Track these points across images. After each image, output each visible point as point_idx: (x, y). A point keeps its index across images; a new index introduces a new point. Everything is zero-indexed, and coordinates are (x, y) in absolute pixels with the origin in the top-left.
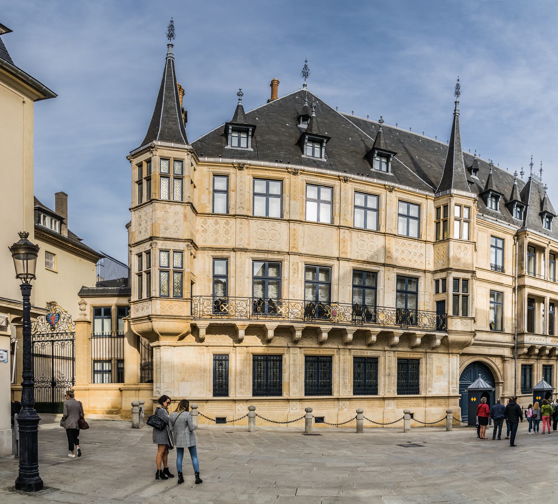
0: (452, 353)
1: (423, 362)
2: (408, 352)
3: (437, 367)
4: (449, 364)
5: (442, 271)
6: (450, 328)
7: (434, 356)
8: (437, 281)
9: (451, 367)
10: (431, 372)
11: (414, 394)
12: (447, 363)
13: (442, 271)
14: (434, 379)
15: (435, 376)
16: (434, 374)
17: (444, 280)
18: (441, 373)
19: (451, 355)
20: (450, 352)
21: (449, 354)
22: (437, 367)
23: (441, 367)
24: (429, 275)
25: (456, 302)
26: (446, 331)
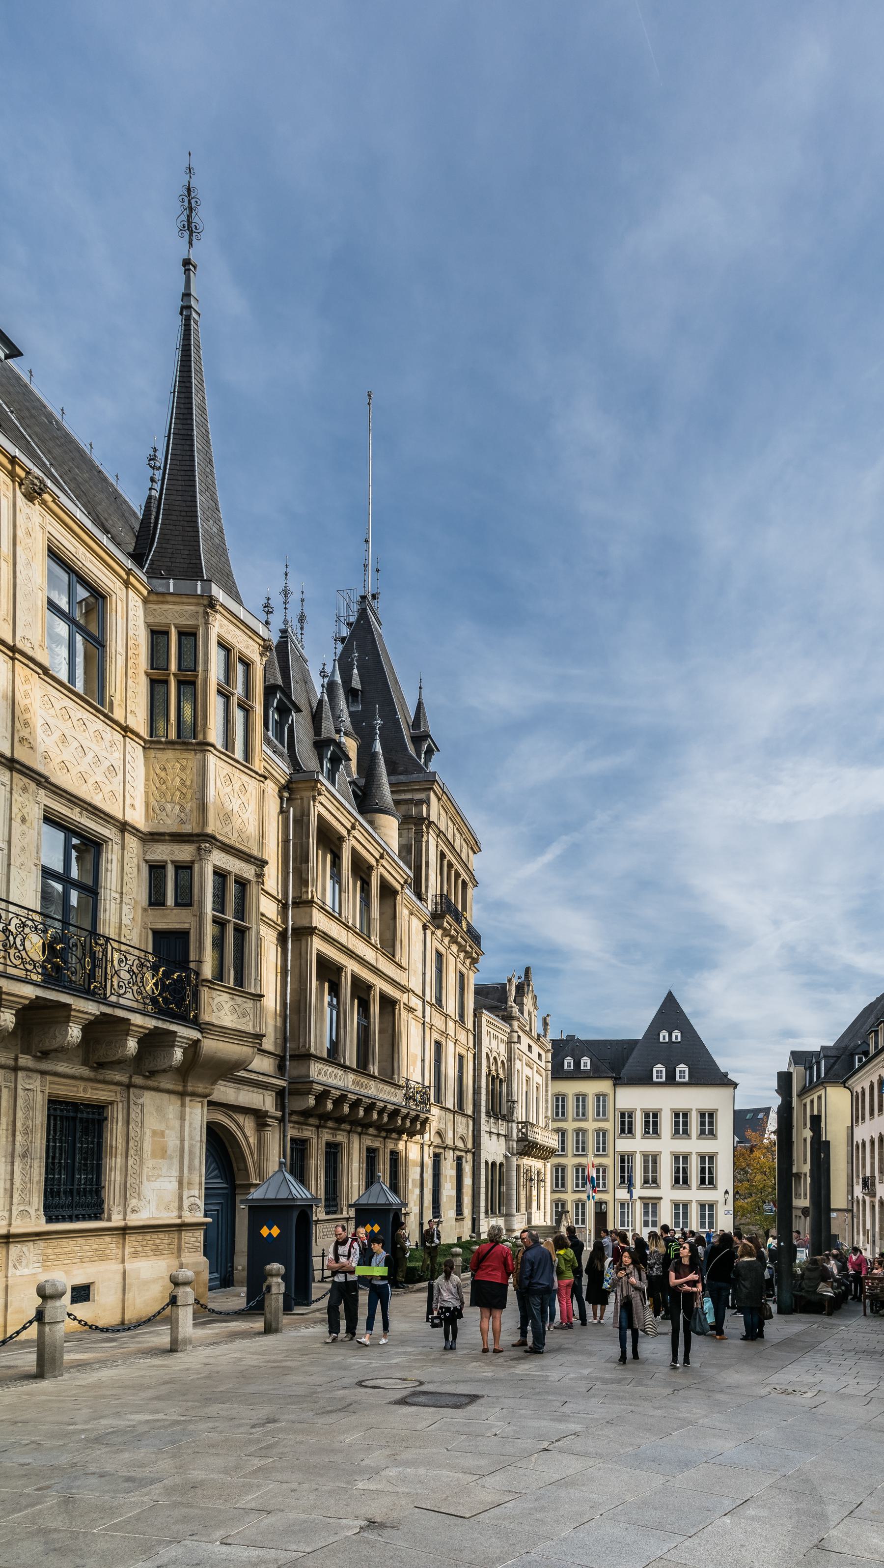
0: (193, 1094)
1: (118, 1114)
2: (82, 1078)
3: (154, 1133)
4: (182, 1127)
5: (178, 838)
6: (206, 1017)
7: (148, 1099)
8: (156, 870)
9: (187, 1138)
10: (140, 1150)
11: (89, 1218)
12: (177, 1123)
13: (178, 838)
14: (145, 1170)
15: (149, 1163)
16: (145, 1156)
17: (184, 869)
18: (162, 1152)
19: (188, 1099)
20: (190, 1089)
21: (182, 1094)
22: (154, 1133)
23: (162, 1134)
24: (132, 842)
25: (219, 943)
26: (196, 1023)
